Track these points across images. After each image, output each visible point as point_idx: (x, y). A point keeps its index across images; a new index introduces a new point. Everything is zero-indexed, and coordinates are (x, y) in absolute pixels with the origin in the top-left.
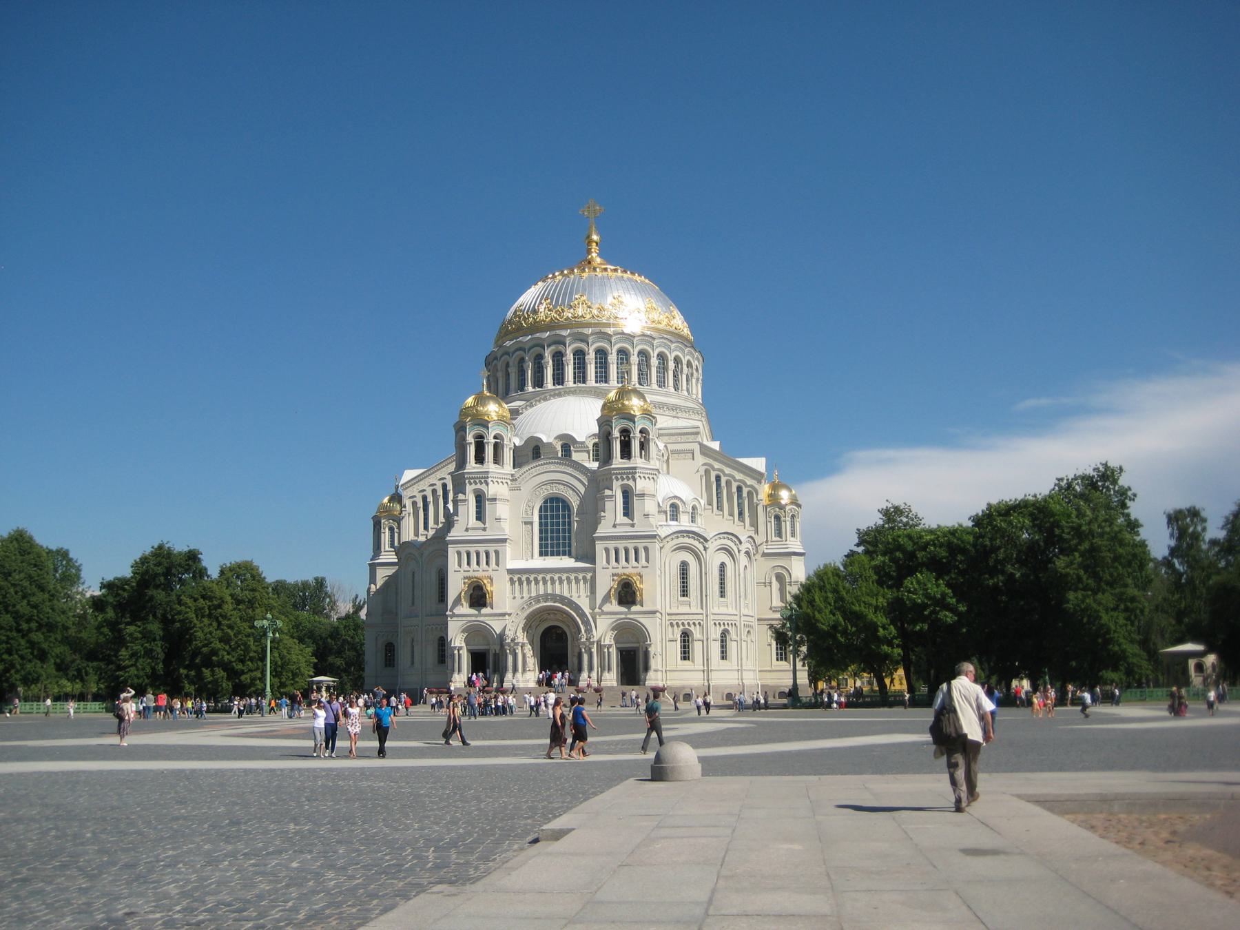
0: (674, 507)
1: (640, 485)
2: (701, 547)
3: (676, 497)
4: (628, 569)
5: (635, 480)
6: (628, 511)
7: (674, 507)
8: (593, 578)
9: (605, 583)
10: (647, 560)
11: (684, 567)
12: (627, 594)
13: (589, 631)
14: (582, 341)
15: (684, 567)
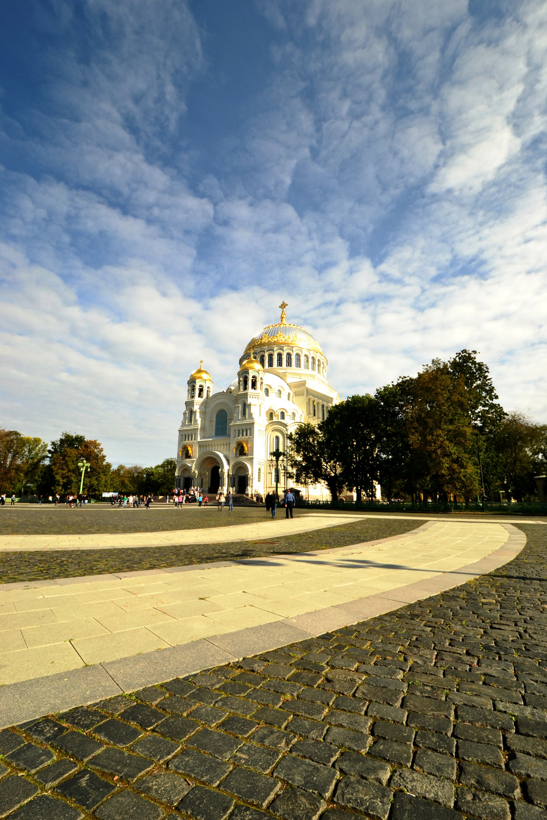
0: (283, 413)
1: (250, 400)
2: (285, 429)
3: (283, 409)
4: (241, 438)
5: (247, 397)
6: (244, 414)
7: (283, 413)
8: (229, 443)
9: (233, 445)
10: (250, 435)
11: (277, 438)
12: (241, 451)
13: (223, 467)
14: (262, 351)
15: (277, 438)
